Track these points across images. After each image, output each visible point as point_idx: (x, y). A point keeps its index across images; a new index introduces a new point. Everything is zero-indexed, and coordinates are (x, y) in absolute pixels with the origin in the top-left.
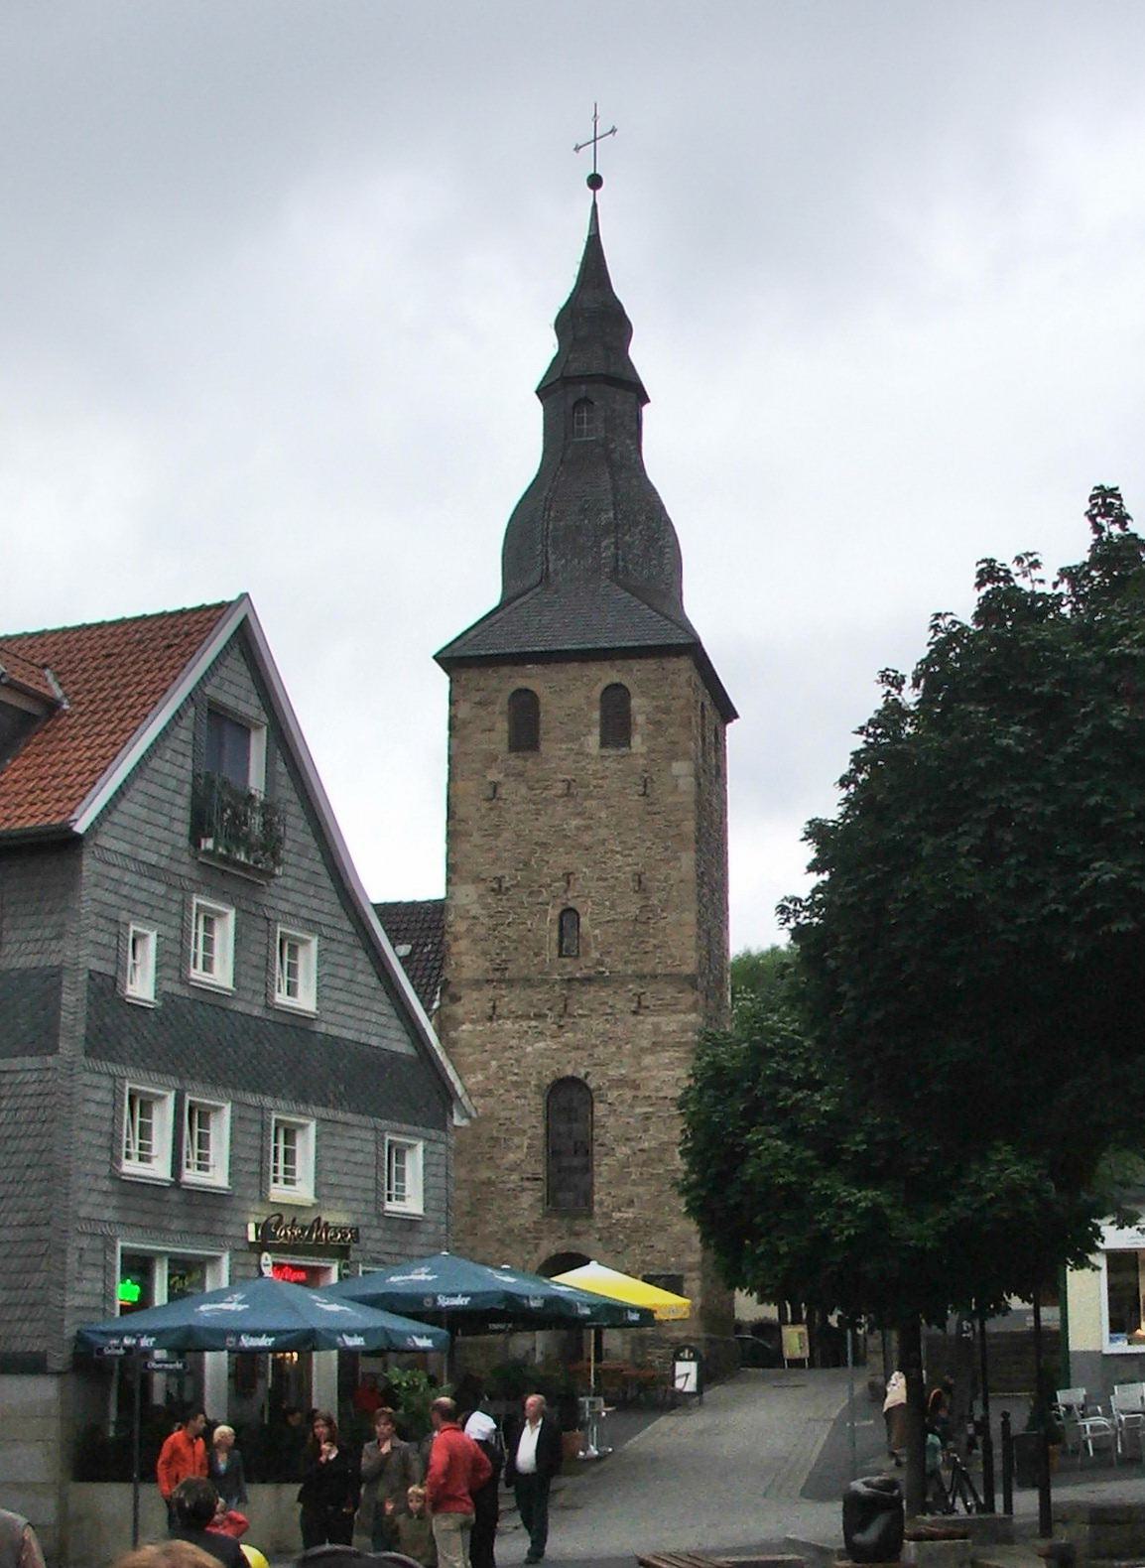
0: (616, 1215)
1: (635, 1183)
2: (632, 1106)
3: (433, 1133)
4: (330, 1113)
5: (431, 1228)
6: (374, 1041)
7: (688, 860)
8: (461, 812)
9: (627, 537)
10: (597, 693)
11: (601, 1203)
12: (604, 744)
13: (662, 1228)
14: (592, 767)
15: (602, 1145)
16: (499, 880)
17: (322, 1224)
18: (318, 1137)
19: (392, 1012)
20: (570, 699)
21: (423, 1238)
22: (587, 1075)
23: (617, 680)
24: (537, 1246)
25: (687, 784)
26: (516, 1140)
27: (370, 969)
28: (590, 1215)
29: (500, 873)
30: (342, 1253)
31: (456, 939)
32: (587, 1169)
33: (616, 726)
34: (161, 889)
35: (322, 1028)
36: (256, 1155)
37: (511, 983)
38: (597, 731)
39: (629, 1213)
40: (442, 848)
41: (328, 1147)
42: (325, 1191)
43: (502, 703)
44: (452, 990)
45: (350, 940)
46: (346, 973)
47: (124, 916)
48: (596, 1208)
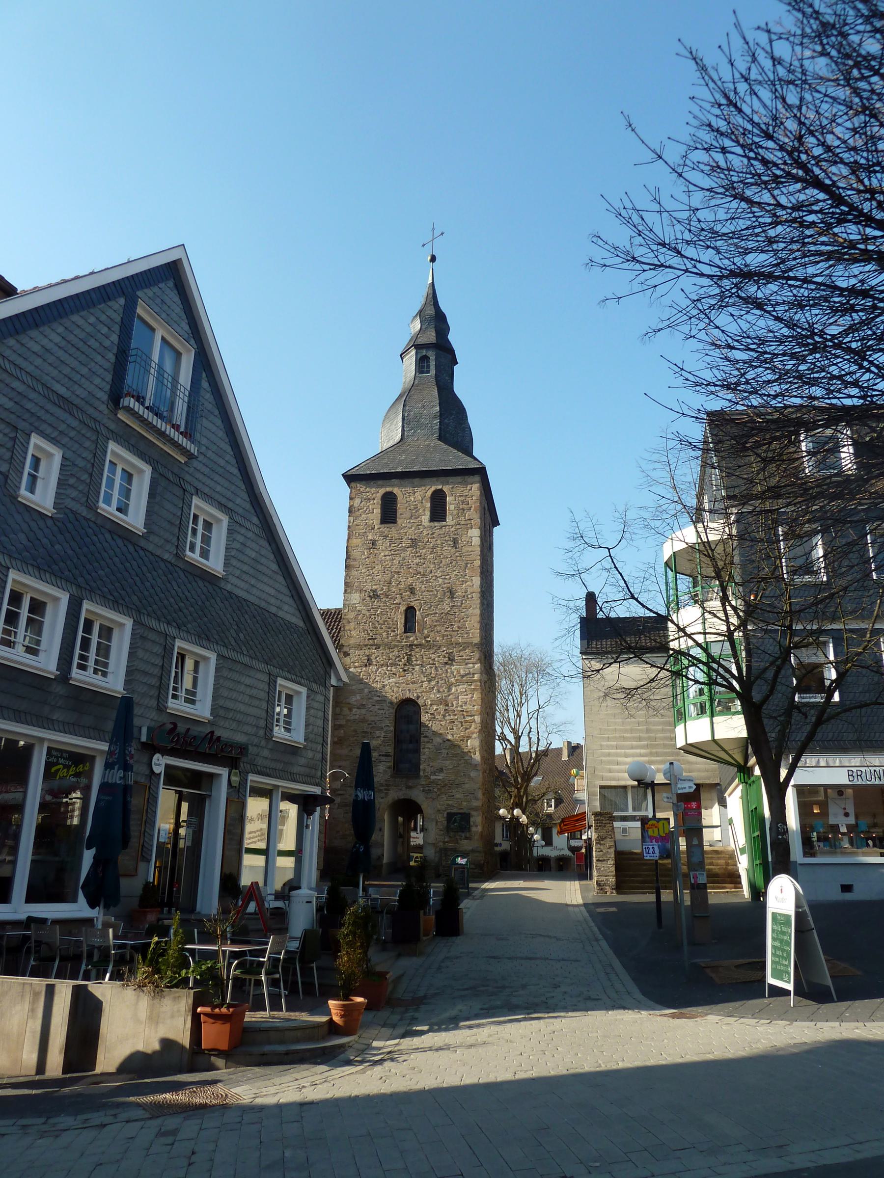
0: (433, 777)
1: (445, 759)
2: (444, 716)
3: (315, 686)
4: (233, 655)
5: (310, 754)
6: (273, 610)
7: (477, 581)
8: (355, 554)
9: (446, 421)
10: (429, 493)
11: (424, 770)
12: (433, 519)
13: (459, 785)
14: (425, 533)
15: (426, 737)
16: (375, 591)
17: (214, 738)
18: (217, 670)
19: (288, 592)
20: (414, 499)
21: (302, 761)
22: (418, 697)
23: (440, 487)
24: (386, 794)
25: (476, 541)
26: (377, 732)
27: (272, 557)
28: (418, 776)
29: (374, 587)
30: (232, 763)
31: (349, 622)
32: (417, 751)
33: (438, 511)
34: (75, 423)
35: (229, 587)
36: (156, 671)
37: (378, 647)
38: (428, 513)
39: (440, 777)
40: (343, 574)
41: (226, 678)
42: (222, 712)
43: (378, 501)
44: (345, 649)
45: (256, 530)
46: (253, 555)
47: (22, 425)
48: (421, 773)
